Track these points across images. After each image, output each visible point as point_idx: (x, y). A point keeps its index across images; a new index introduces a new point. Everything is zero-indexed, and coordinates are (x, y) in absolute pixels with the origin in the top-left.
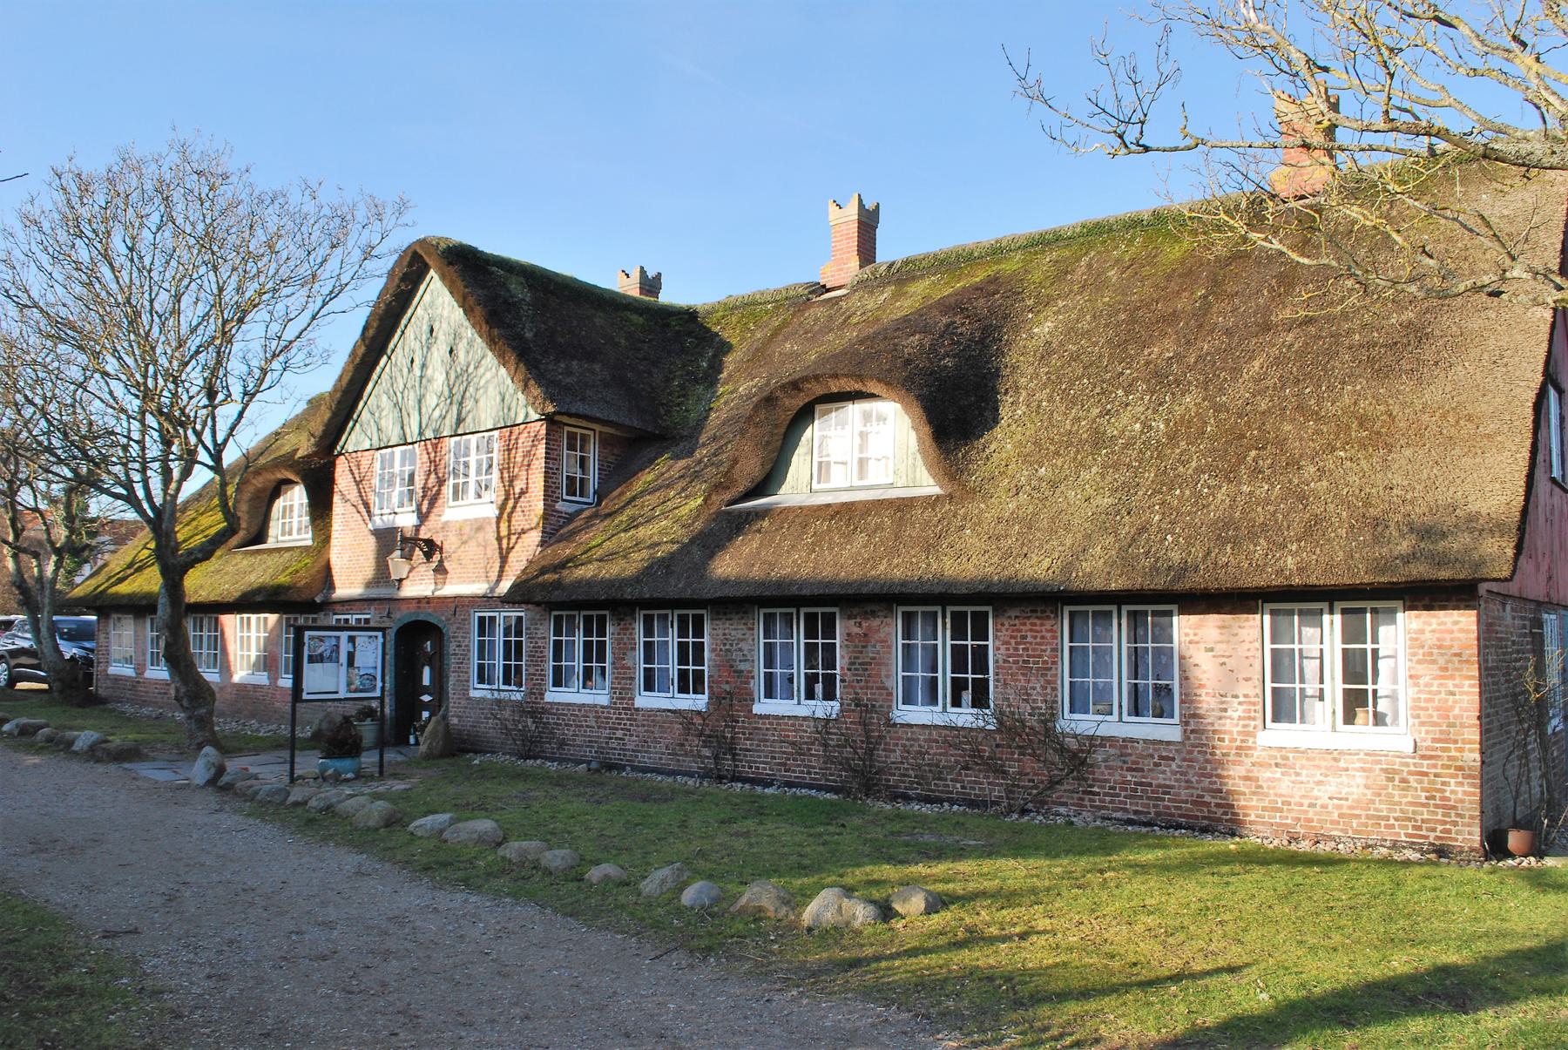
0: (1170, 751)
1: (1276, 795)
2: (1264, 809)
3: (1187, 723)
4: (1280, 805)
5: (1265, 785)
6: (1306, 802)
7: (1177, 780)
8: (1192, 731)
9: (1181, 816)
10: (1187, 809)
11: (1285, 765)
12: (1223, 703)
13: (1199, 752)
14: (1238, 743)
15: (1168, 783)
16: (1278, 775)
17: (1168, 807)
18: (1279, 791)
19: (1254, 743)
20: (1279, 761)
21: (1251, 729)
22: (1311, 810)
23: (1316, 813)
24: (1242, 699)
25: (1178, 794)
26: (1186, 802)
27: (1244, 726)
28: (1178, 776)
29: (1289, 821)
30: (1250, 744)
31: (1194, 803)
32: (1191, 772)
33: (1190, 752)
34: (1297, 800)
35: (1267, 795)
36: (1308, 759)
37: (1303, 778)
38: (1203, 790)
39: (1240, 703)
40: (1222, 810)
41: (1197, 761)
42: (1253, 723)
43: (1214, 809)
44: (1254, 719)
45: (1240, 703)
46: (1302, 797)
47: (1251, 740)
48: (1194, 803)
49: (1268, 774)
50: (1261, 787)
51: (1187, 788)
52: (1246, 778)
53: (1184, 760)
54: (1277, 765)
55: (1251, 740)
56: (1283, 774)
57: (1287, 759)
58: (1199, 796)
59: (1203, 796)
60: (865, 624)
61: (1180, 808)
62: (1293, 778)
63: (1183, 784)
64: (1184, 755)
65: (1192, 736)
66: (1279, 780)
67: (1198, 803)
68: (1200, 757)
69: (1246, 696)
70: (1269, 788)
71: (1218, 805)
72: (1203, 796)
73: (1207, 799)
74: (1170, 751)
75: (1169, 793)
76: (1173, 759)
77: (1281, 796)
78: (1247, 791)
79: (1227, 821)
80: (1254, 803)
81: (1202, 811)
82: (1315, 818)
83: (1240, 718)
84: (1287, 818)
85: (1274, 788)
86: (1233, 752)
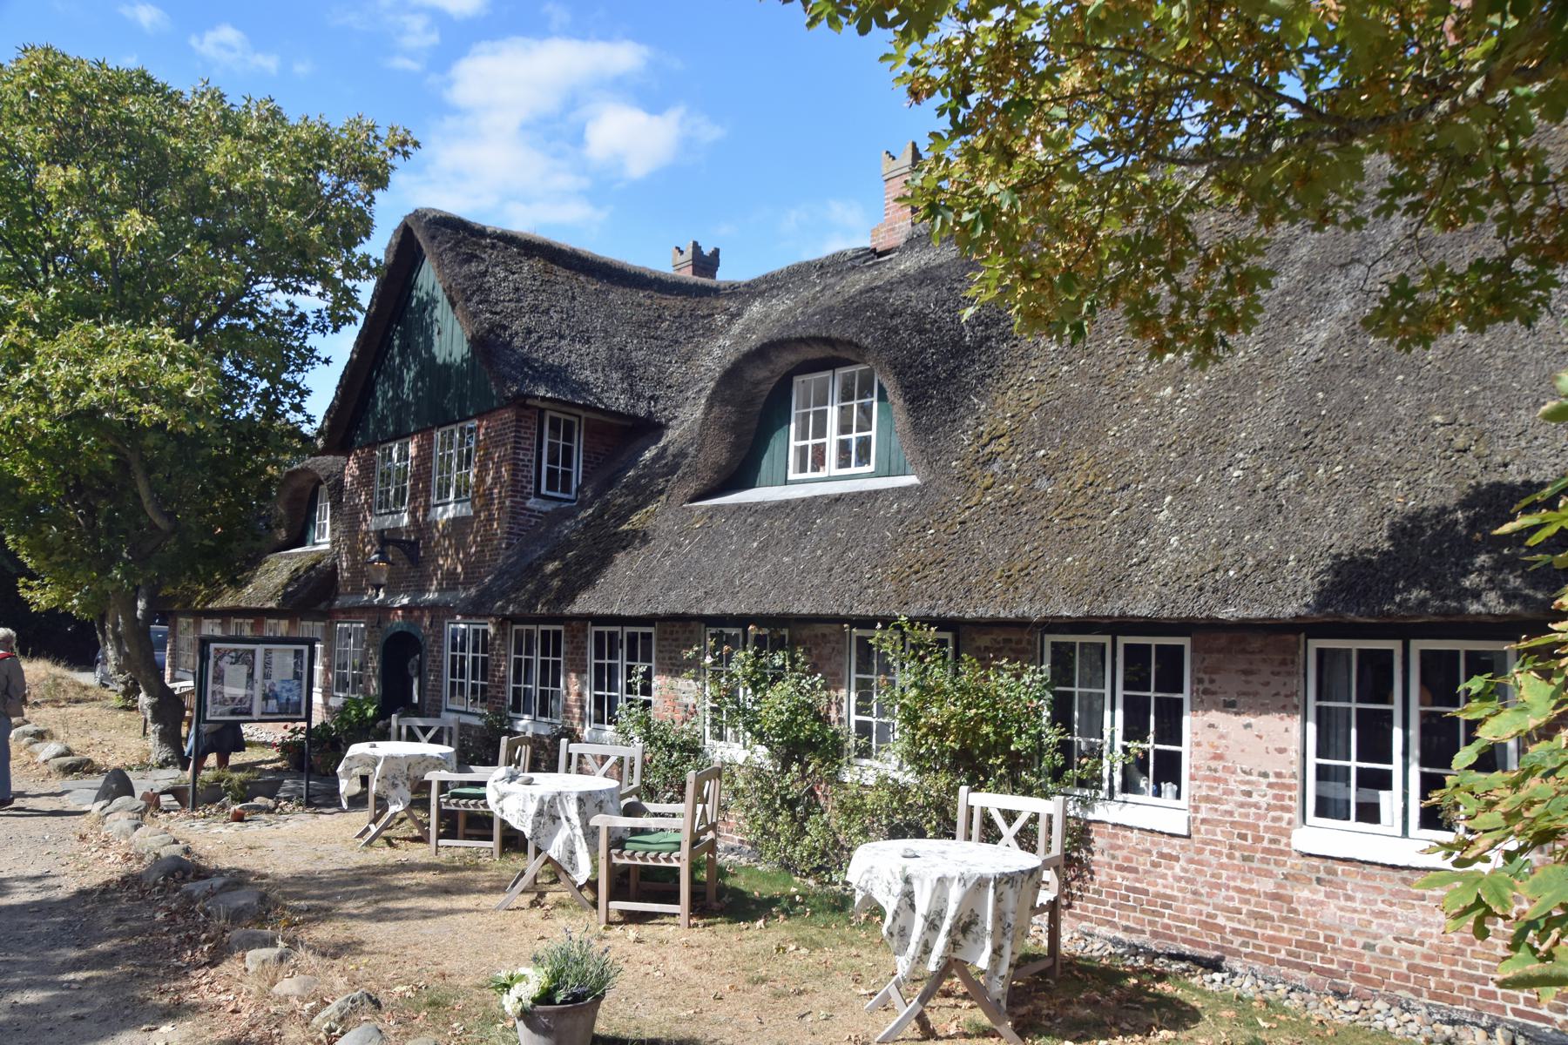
0: (1173, 847)
1: (1316, 925)
2: (1299, 944)
3: (1196, 809)
4: (1321, 941)
5: (1300, 909)
6: (1360, 941)
7: (1181, 890)
8: (1204, 821)
9: (1185, 941)
10: (1193, 933)
11: (1330, 882)
12: (1248, 783)
13: (1212, 852)
14: (1265, 844)
15: (1169, 892)
16: (1321, 897)
17: (1167, 927)
18: (1321, 921)
19: (1288, 845)
20: (1322, 875)
21: (1284, 824)
22: (1367, 953)
23: (1374, 959)
24: (1272, 779)
25: (1183, 910)
26: (1193, 922)
27: (1275, 819)
28: (1183, 884)
29: (1335, 967)
30: (1282, 847)
31: (1203, 924)
32: (1200, 879)
33: (1200, 851)
34: (1347, 935)
35: (1304, 924)
36: (1365, 877)
37: (1357, 905)
38: (1216, 907)
39: (1270, 785)
40: (1240, 939)
41: (1210, 865)
42: (1286, 816)
43: (1229, 937)
44: (1288, 809)
45: (1270, 785)
46: (1354, 932)
47: (1284, 840)
48: (1203, 924)
49: (1306, 894)
50: (1294, 911)
51: (1195, 902)
52: (1276, 897)
53: (1191, 861)
54: (1319, 880)
55: (1284, 840)
56: (1327, 895)
57: (1335, 873)
58: (1209, 915)
59: (1214, 917)
60: (814, 652)
61: (1184, 930)
62: (1342, 903)
63: (1189, 896)
64: (1191, 854)
65: (1203, 828)
66: (1322, 903)
67: (1209, 926)
68: (1213, 860)
69: (1278, 775)
70: (1307, 913)
71: (1235, 931)
72: (1214, 917)
73: (1221, 920)
74: (1173, 847)
75: (1169, 907)
76: (1177, 859)
77: (1324, 927)
78: (1276, 914)
79: (1246, 955)
80: (1285, 934)
81: (1212, 937)
82: (1373, 966)
83: (1269, 808)
84: (1332, 961)
85: (1314, 914)
86: (1258, 855)
